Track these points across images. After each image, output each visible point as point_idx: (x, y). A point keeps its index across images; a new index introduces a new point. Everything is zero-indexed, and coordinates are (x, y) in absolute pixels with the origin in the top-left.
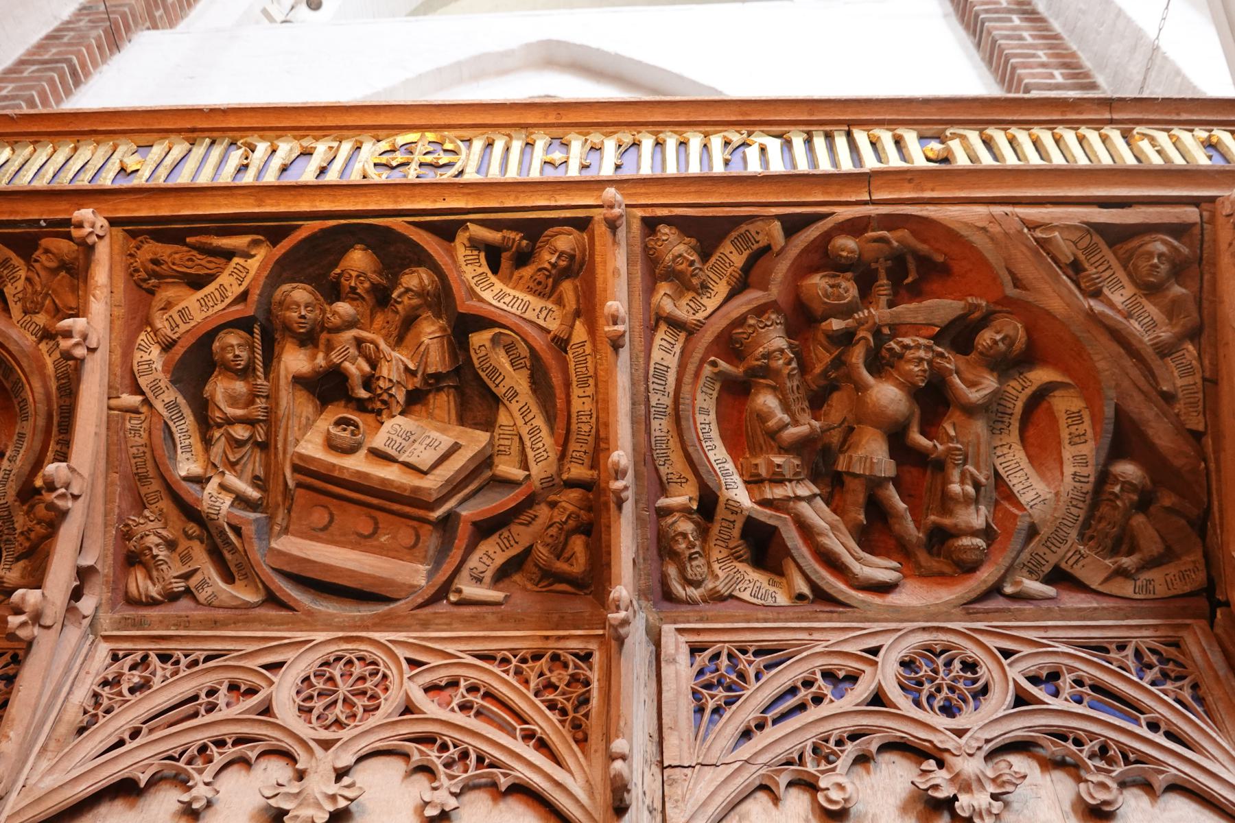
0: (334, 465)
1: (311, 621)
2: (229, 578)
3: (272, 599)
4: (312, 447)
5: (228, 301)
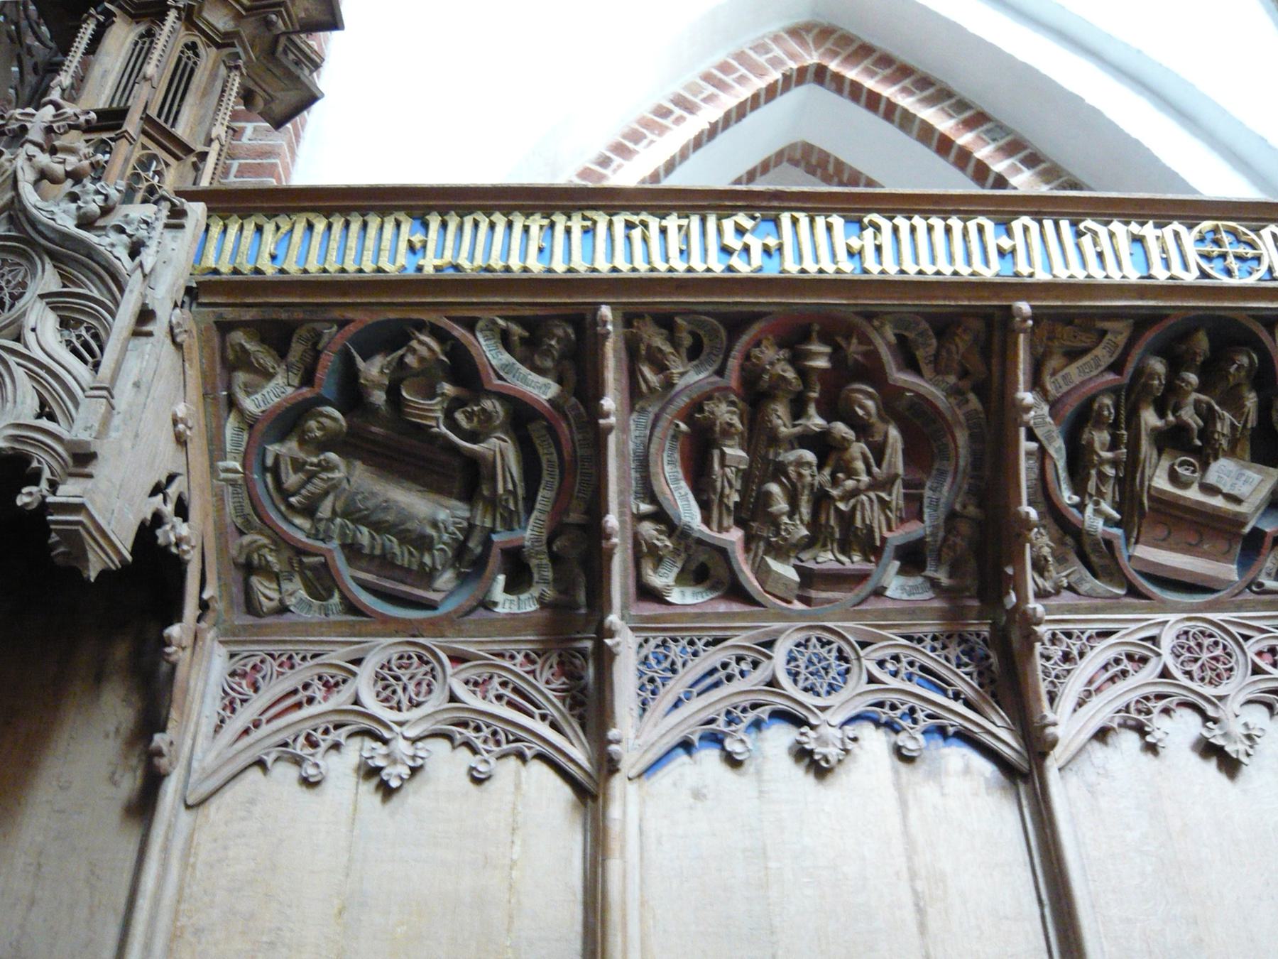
0: (1180, 496)
1: (1165, 607)
2: (1095, 575)
3: (1134, 592)
4: (1161, 482)
5: (1100, 369)
